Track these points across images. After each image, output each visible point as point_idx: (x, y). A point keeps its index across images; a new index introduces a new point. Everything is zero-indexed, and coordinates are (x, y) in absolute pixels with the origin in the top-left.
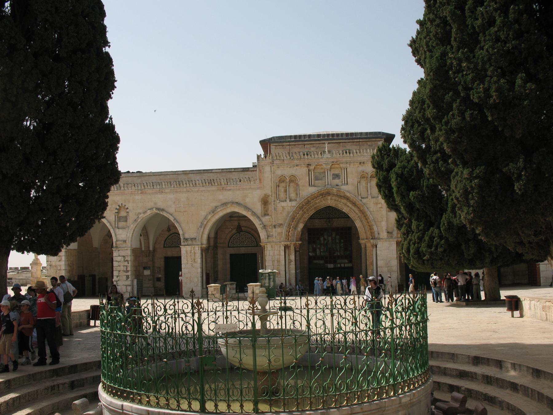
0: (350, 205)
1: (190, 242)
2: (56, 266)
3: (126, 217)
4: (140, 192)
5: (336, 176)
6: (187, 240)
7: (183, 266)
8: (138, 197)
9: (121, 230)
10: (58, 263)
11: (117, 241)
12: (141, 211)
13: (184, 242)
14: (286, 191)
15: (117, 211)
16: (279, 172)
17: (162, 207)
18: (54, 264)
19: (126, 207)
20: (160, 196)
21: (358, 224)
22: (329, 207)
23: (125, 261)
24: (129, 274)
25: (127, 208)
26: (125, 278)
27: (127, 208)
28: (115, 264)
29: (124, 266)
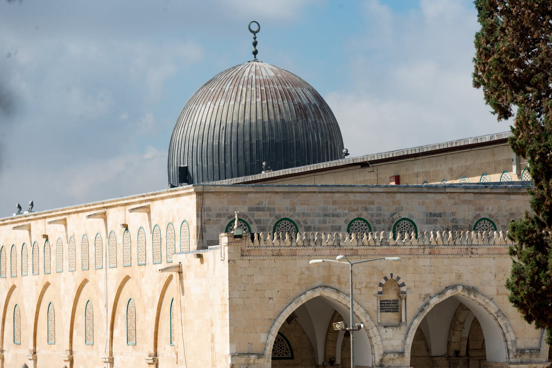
1: (526, 357)
3: (396, 302)
4: (427, 251)
8: (425, 262)
9: (390, 330)
11: (385, 353)
12: (431, 291)
13: (515, 356)
15: (381, 289)
17: (471, 284)
19: (400, 282)
20: (466, 261)
25: (403, 285)
27: (403, 285)
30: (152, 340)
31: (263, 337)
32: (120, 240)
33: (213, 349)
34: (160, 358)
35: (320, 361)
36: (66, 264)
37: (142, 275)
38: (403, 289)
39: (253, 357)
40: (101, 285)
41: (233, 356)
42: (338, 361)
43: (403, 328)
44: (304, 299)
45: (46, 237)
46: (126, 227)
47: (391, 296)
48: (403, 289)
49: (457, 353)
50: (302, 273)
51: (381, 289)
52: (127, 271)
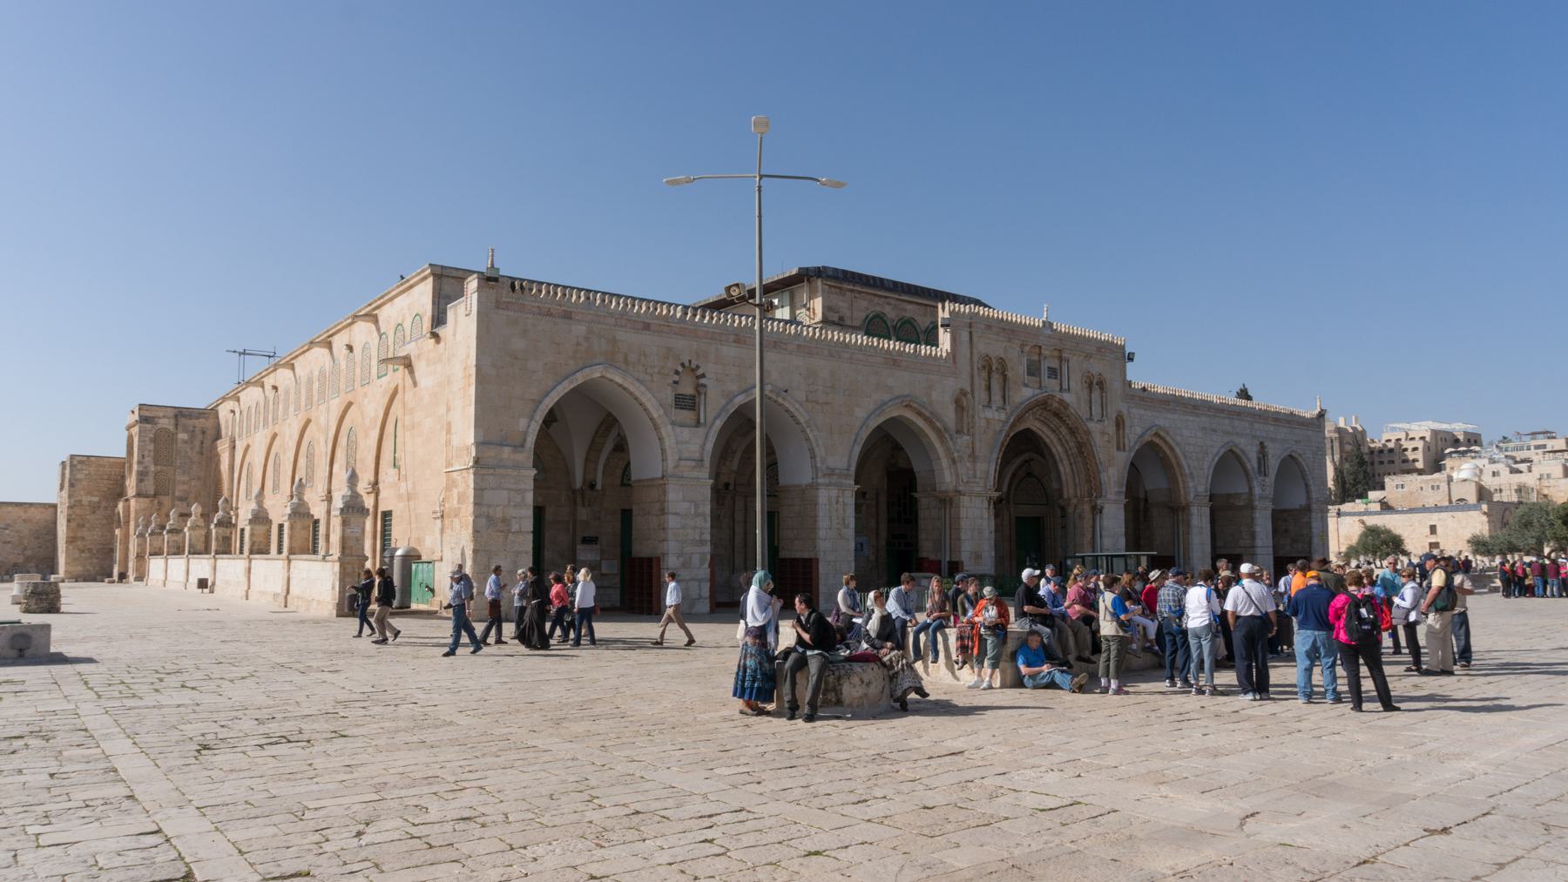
0: (1064, 430)
2: (505, 520)
3: (693, 397)
5: (1053, 373)
6: (831, 472)
7: (822, 533)
10: (512, 512)
12: (734, 387)
14: (989, 388)
15: (676, 378)
16: (982, 347)
18: (499, 515)
19: (700, 372)
21: (1065, 468)
22: (1028, 430)
23: (697, 515)
24: (707, 549)
25: (703, 376)
26: (696, 560)
27: (703, 376)
28: (672, 522)
29: (695, 528)
30: (373, 466)
31: (523, 422)
32: (343, 366)
33: (448, 442)
34: (381, 486)
35: (578, 484)
36: (291, 409)
37: (365, 395)
38: (702, 381)
39: (507, 450)
40: (322, 420)
41: (478, 444)
42: (599, 487)
43: (701, 430)
44: (580, 378)
45: (275, 388)
46: (350, 348)
47: (688, 390)
48: (702, 381)
49: (727, 485)
50: (578, 344)
51: (676, 378)
52: (350, 397)
